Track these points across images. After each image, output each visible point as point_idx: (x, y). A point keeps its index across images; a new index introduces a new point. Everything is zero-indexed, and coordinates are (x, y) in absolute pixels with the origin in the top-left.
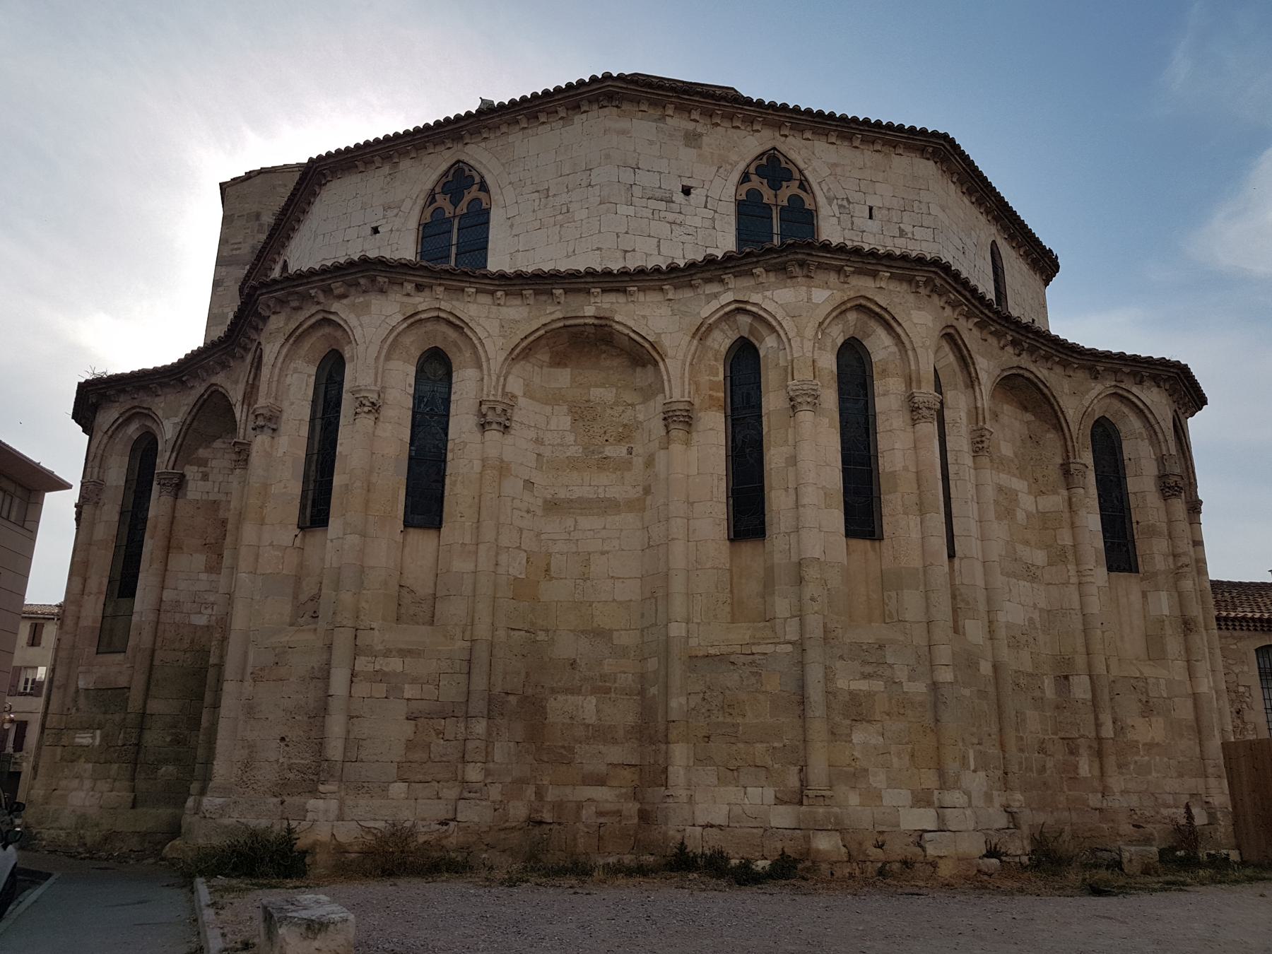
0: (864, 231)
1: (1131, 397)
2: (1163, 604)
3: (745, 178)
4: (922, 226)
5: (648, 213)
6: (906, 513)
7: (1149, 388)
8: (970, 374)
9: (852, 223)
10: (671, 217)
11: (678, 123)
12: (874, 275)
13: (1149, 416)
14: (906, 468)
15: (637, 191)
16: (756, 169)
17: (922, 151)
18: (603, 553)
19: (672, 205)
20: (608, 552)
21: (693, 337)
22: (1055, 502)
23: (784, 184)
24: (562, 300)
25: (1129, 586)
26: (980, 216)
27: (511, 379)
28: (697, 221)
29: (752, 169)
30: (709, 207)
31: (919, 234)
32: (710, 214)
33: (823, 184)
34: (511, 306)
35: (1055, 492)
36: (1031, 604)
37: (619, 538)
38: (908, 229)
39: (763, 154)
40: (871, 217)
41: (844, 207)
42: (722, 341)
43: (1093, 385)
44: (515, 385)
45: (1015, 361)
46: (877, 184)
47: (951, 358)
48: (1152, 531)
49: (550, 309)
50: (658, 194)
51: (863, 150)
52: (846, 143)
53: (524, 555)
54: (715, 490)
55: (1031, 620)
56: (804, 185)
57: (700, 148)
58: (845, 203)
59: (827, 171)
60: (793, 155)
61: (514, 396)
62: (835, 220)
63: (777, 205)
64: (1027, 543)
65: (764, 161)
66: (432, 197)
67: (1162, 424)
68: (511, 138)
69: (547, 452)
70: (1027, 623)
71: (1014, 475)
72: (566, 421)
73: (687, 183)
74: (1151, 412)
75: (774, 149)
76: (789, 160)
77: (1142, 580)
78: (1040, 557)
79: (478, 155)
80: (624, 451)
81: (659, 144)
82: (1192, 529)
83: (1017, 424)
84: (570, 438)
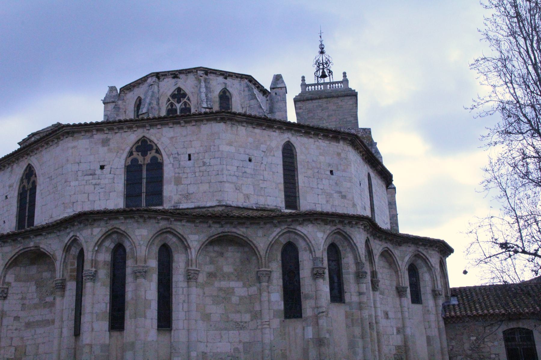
0: (185, 167)
1: (296, 231)
2: (310, 333)
3: (131, 153)
4: (215, 158)
5: (84, 183)
6: (131, 318)
7: (307, 225)
8: (185, 244)
9: (180, 164)
10: (94, 182)
11: (99, 136)
12: (117, 218)
13: (307, 239)
14: (132, 299)
15: (80, 174)
16: (137, 148)
17: (215, 120)
18: (43, 343)
19: (95, 176)
20: (44, 343)
21: (64, 250)
22: (254, 290)
23: (149, 152)
24: (23, 241)
25: (295, 325)
26: (274, 133)
27: (7, 276)
28: (107, 181)
29: (134, 149)
30: (112, 172)
31: (213, 162)
32: (111, 176)
33: (166, 150)
34: (6, 246)
35: (254, 285)
36: (238, 340)
37: (49, 336)
38: (207, 160)
39: (139, 140)
40: (190, 159)
41: (175, 158)
42: (74, 251)
43: (275, 229)
44: (10, 278)
45: (220, 230)
46: (193, 142)
47: (174, 239)
48: (307, 297)
49: (19, 245)
50: (90, 172)
51: (187, 127)
52: (178, 125)
53: (13, 349)
54: (70, 315)
55: (237, 350)
56: (158, 151)
57: (109, 145)
58: (176, 155)
59: (169, 142)
60: (153, 138)
61: (9, 284)
62: (171, 165)
63: (144, 164)
64: (239, 312)
65: (140, 144)
66: (22, 180)
67: (313, 242)
68: (43, 153)
69: (27, 302)
70: (232, 351)
71: (233, 280)
72: (33, 288)
73: (102, 164)
74: (308, 238)
75: (144, 137)
76: (151, 141)
77: (303, 321)
78: (247, 317)
79: (34, 160)
80: (52, 298)
81: (90, 149)
82: (359, 287)
83: (239, 255)
84: (35, 295)
